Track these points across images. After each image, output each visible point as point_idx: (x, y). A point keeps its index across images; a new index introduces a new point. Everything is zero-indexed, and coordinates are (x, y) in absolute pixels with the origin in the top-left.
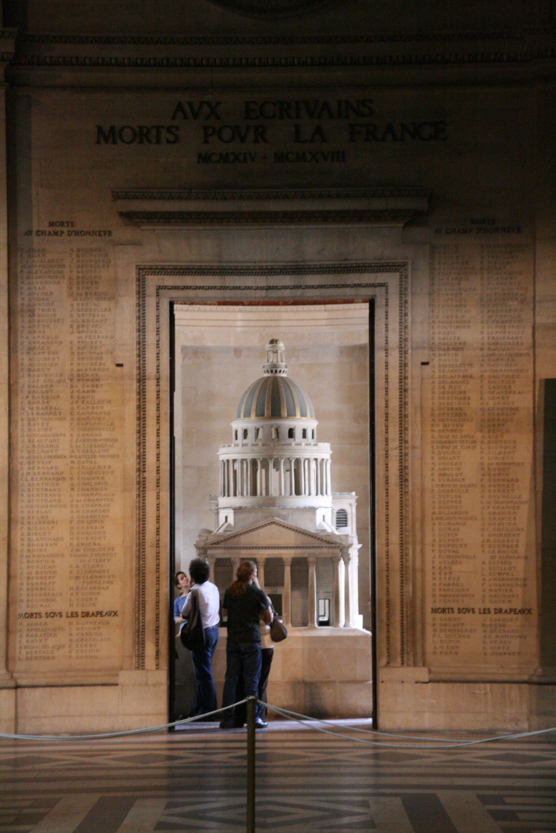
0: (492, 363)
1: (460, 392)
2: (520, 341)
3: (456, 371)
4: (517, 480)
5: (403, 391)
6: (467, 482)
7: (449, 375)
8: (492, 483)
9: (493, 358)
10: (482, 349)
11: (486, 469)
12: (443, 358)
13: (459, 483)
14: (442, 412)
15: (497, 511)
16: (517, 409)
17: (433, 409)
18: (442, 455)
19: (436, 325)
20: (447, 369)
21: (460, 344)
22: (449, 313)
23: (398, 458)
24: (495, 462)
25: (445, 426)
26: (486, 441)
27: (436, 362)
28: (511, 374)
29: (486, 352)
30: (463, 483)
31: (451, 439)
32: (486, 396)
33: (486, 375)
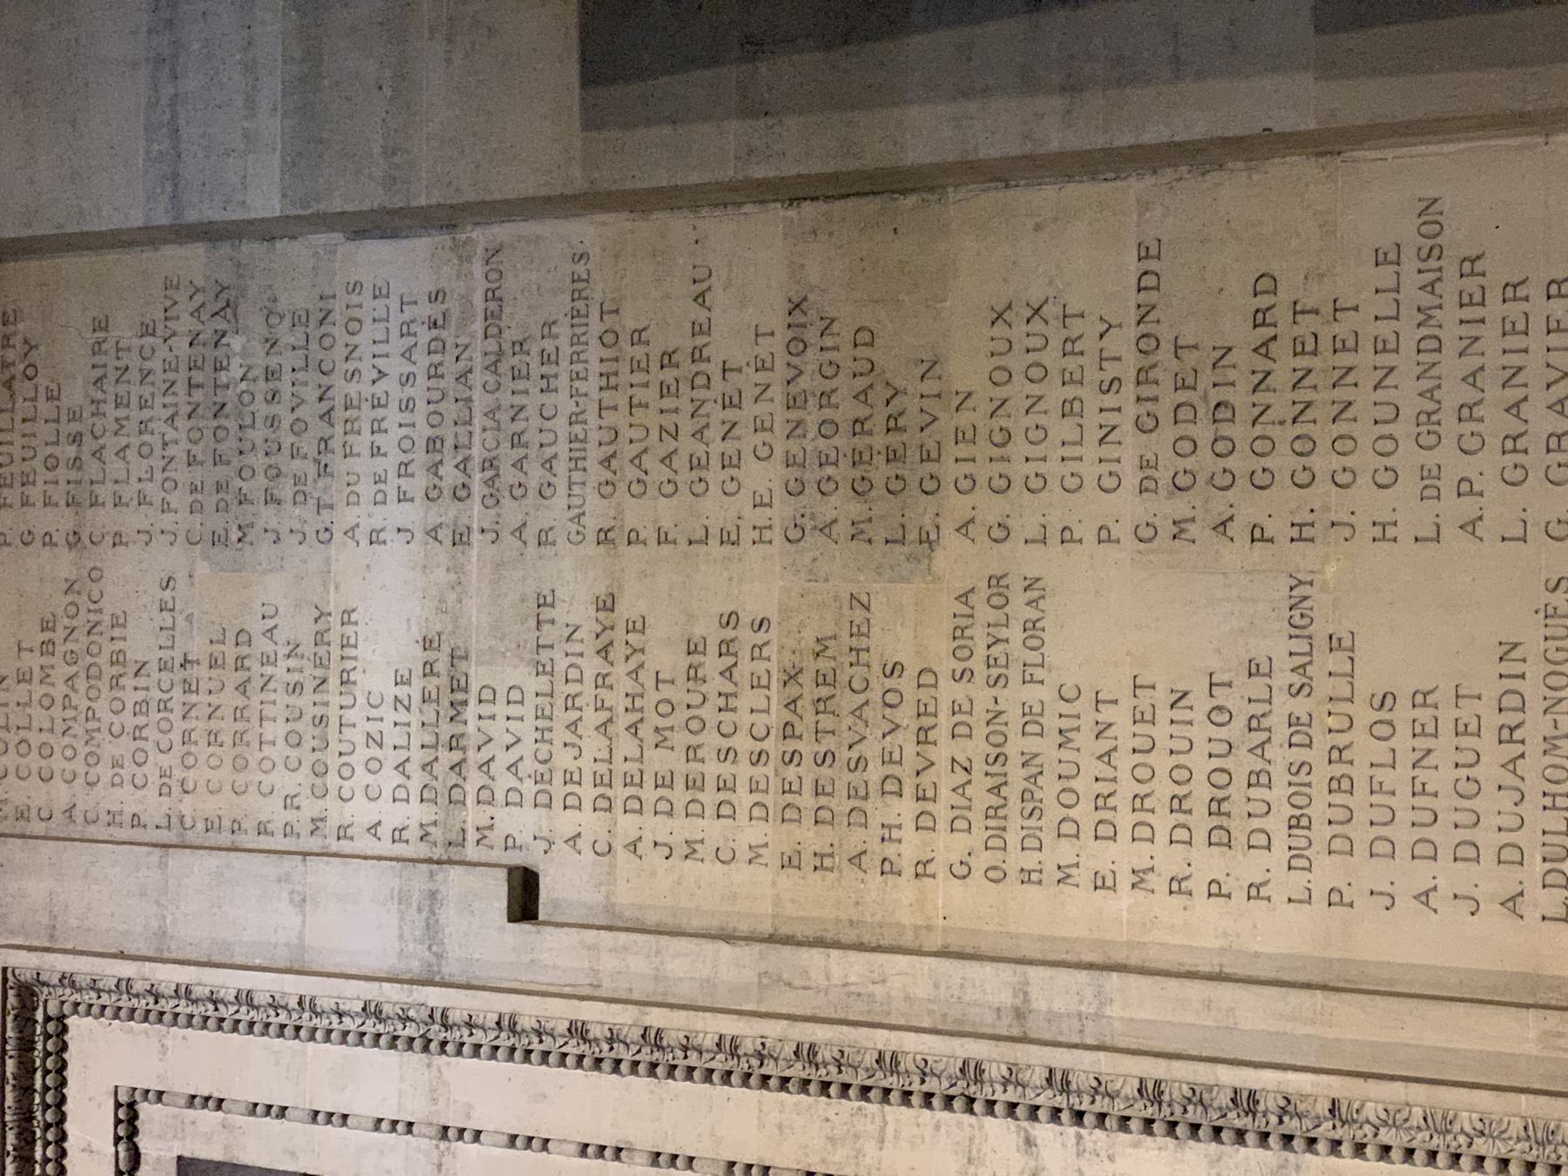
0: (535, 475)
1: (694, 675)
2: (425, 310)
3: (571, 702)
4: (1265, 283)
5: (657, 1057)
6: (1276, 646)
7: (594, 744)
8: (1282, 462)
9: (509, 475)
10: (460, 539)
11: (1180, 507)
12: (504, 781)
13: (1283, 706)
14: (807, 801)
15: (1496, 423)
16: (796, 306)
17: (790, 862)
18: (1084, 813)
19: (337, 814)
20: (564, 759)
21: (429, 670)
22: (275, 730)
23: (1095, 1138)
24: (1130, 448)
25: (891, 787)
26: (990, 508)
27: (521, 827)
28: (594, 352)
29: (475, 513)
30: (1283, 678)
31: (976, 748)
32: (716, 510)
33: (597, 511)
